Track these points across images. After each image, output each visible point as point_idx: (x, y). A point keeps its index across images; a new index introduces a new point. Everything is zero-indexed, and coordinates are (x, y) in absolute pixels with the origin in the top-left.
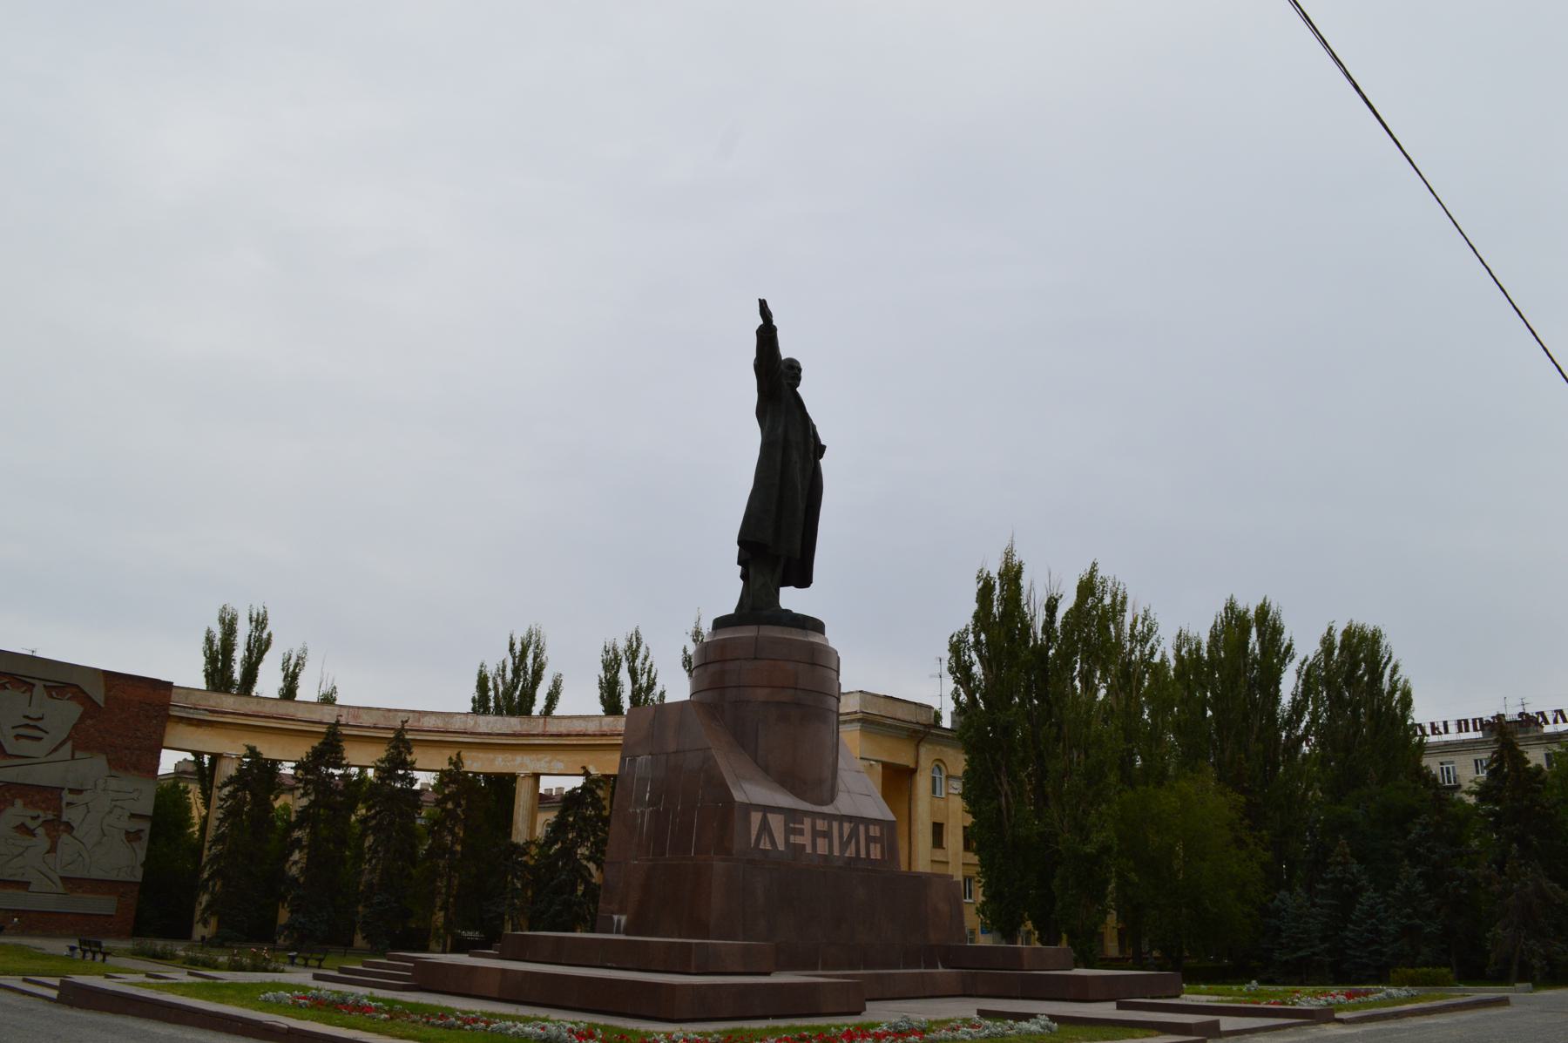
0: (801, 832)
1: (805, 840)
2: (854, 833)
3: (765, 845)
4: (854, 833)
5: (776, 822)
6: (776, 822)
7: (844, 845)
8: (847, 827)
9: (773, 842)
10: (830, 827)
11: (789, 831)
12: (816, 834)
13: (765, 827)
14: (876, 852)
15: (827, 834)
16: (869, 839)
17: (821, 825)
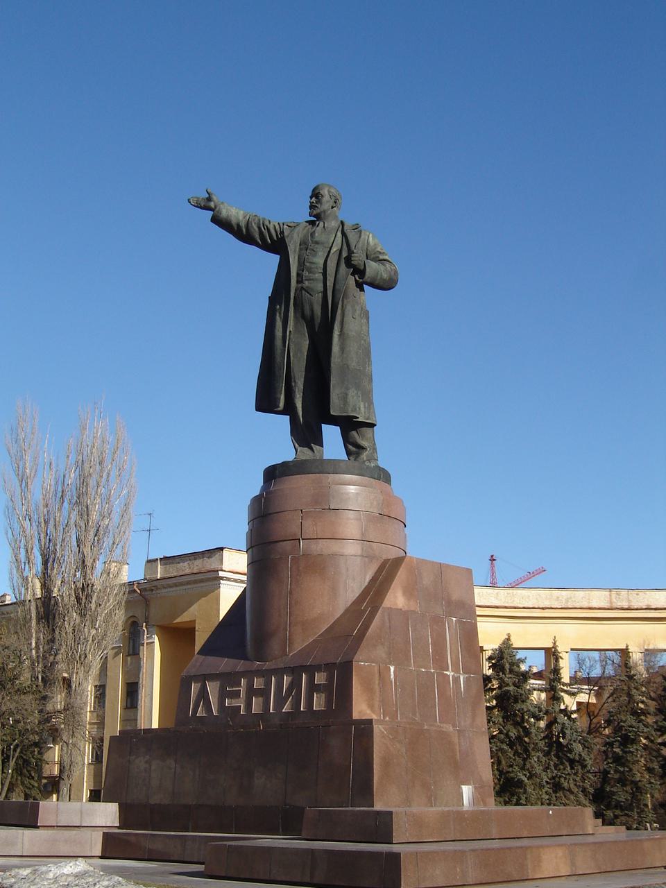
0: (236, 695)
1: (240, 703)
2: (295, 685)
3: (200, 712)
4: (295, 685)
5: (212, 689)
6: (212, 689)
7: (280, 701)
8: (286, 680)
9: (208, 707)
10: (268, 683)
11: (223, 695)
12: (251, 692)
13: (203, 694)
14: (318, 703)
15: (264, 693)
16: (313, 688)
17: (257, 683)
